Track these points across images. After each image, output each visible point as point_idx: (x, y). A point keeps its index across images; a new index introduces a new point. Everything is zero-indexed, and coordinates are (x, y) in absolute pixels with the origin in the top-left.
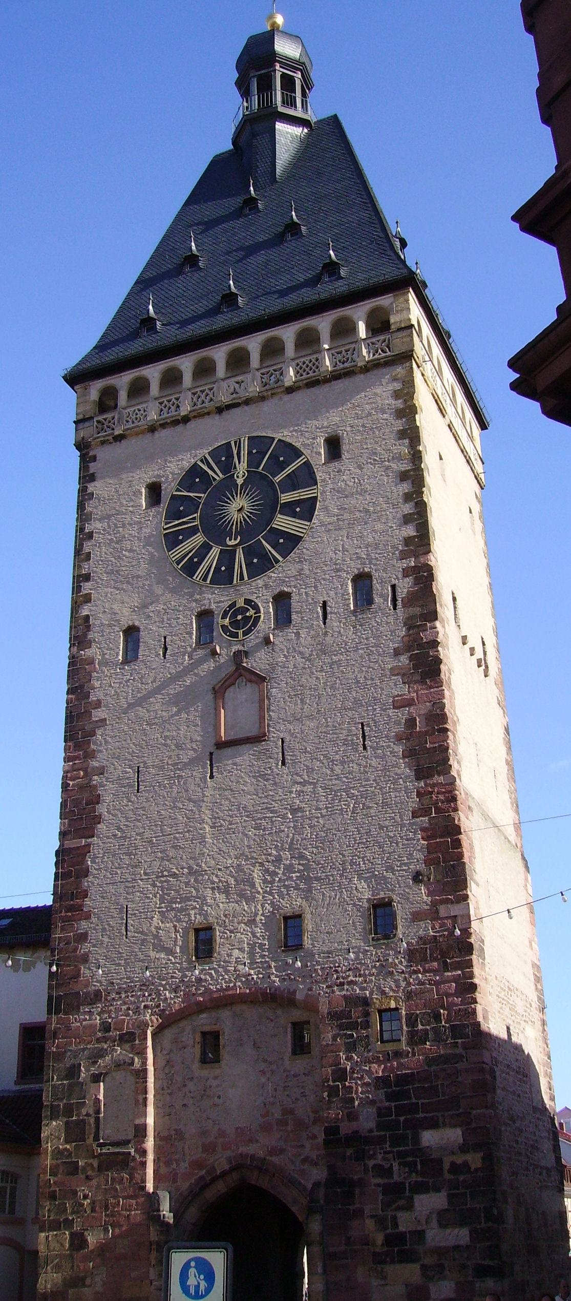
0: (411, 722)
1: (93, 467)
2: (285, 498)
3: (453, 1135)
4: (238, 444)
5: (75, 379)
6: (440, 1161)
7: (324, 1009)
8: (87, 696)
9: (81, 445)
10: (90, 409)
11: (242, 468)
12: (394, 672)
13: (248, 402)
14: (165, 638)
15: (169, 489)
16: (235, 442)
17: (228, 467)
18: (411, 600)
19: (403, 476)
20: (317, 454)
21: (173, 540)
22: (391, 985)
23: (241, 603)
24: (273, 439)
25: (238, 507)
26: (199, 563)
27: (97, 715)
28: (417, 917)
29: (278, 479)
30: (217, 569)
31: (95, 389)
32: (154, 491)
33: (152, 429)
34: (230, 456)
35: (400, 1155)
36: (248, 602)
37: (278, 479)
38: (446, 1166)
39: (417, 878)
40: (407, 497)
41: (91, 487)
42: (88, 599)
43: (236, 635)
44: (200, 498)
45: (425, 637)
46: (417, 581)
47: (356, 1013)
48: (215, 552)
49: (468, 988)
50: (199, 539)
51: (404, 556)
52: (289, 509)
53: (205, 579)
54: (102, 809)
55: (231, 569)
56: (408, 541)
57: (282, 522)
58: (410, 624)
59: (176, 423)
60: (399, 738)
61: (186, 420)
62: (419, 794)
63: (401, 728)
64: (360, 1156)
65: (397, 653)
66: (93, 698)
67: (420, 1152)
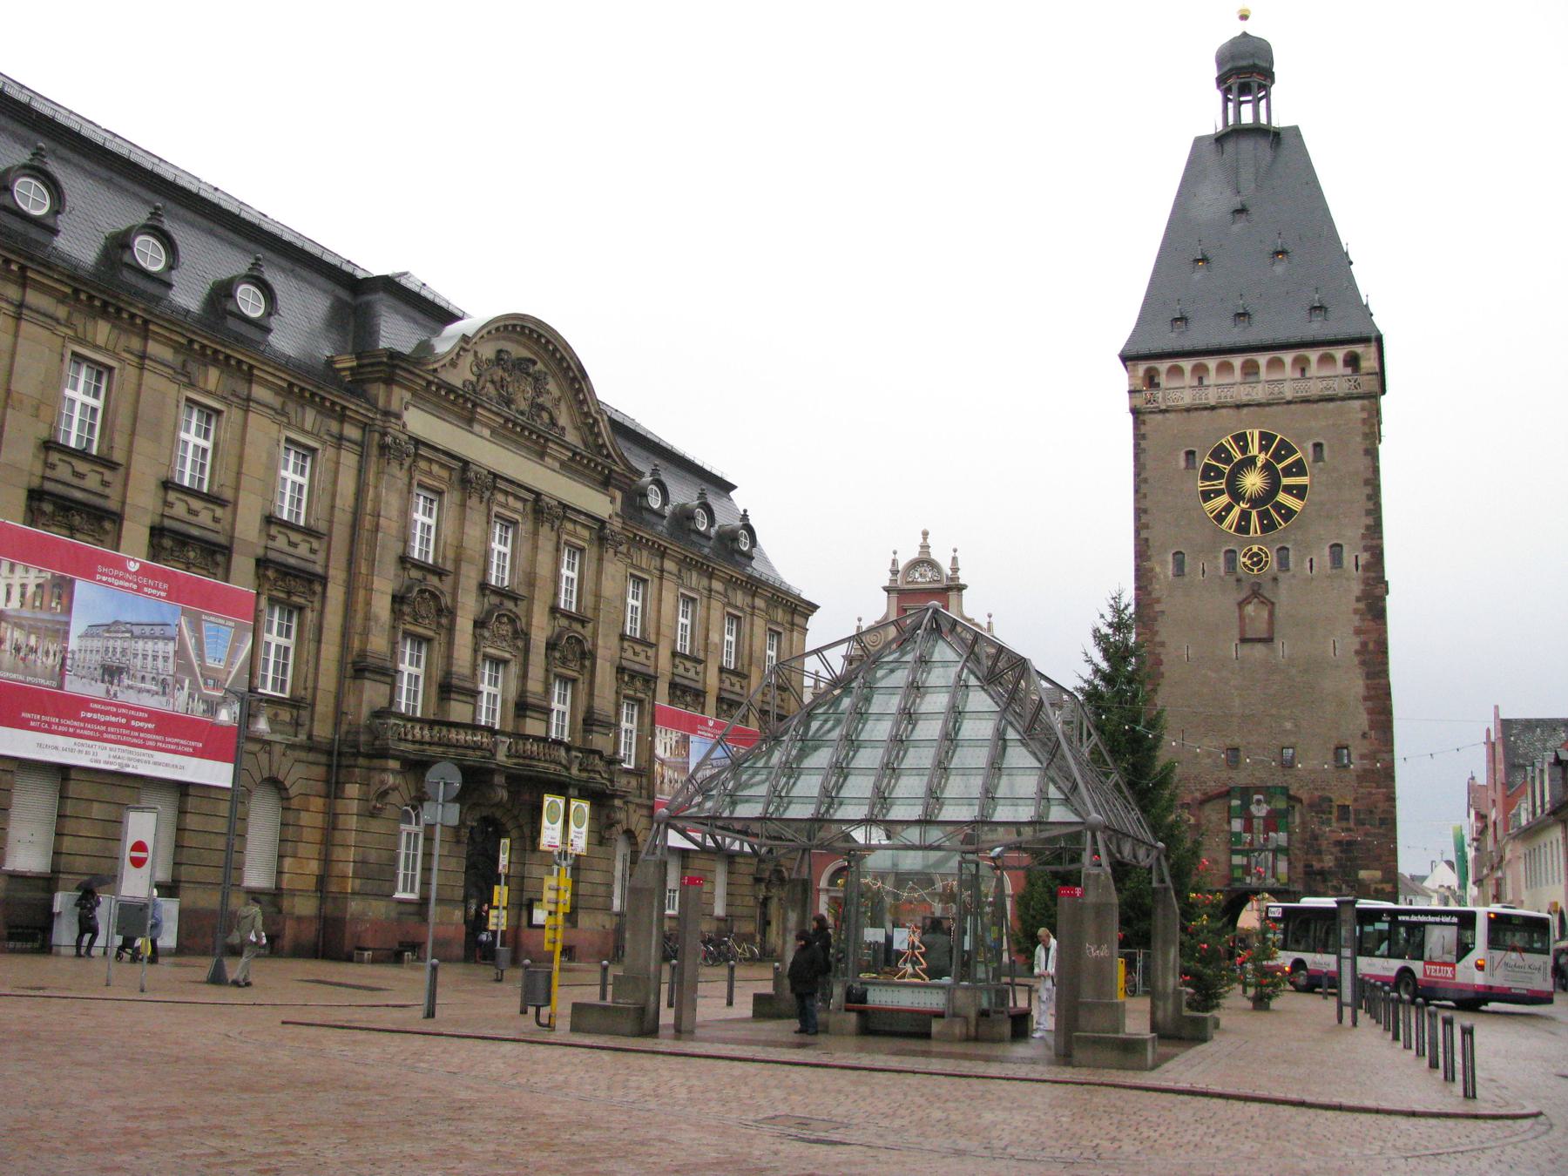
0: (1364, 645)
1: (1143, 429)
2: (1286, 481)
3: (1378, 874)
5: (1127, 358)
6: (1368, 886)
7: (1305, 802)
8: (1150, 594)
9: (1135, 411)
10: (1139, 383)
11: (1254, 449)
12: (1356, 611)
13: (1259, 405)
18: (1367, 568)
19: (1367, 482)
21: (1206, 496)
22: (1344, 795)
23: (1255, 549)
25: (1253, 482)
27: (1157, 608)
28: (1362, 757)
29: (1280, 467)
30: (1239, 523)
31: (1142, 368)
33: (1188, 410)
34: (1247, 445)
35: (1346, 882)
37: (1280, 467)
38: (1373, 887)
39: (1364, 735)
40: (1369, 498)
41: (1143, 444)
42: (1146, 526)
45: (1378, 592)
46: (1373, 555)
47: (1325, 806)
49: (1391, 799)
50: (1225, 499)
51: (1364, 537)
52: (1288, 490)
54: (1162, 669)
55: (1248, 522)
56: (1368, 528)
57: (1282, 497)
58: (1366, 582)
59: (1206, 409)
60: (1357, 652)
61: (1213, 408)
62: (1367, 687)
63: (1357, 647)
64: (1324, 881)
65: (1358, 600)
66: (1154, 595)
67: (1358, 880)
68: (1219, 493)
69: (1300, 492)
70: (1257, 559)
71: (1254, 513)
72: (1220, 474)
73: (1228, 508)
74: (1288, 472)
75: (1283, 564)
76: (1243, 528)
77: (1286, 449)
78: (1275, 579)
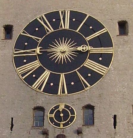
4: (64, 13)
14: (12, 118)
15: (18, 32)
16: (62, 12)
17: (56, 25)
20: (113, 30)
21: (19, 62)
24: (86, 15)
25: (63, 50)
26: (37, 78)
29: (88, 39)
32: (8, 29)
36: (66, 106)
37: (88, 39)
43: (59, 125)
44: (38, 40)
48: (47, 74)
50: (36, 64)
52: (94, 57)
53: (40, 88)
57: (89, 63)
68: (31, 59)
69: (106, 60)
70: (64, 116)
71: (62, 76)
72: (33, 44)
73: (39, 72)
74: (94, 43)
75: (90, 121)
76: (51, 88)
77: (94, 25)
78: (79, 132)
